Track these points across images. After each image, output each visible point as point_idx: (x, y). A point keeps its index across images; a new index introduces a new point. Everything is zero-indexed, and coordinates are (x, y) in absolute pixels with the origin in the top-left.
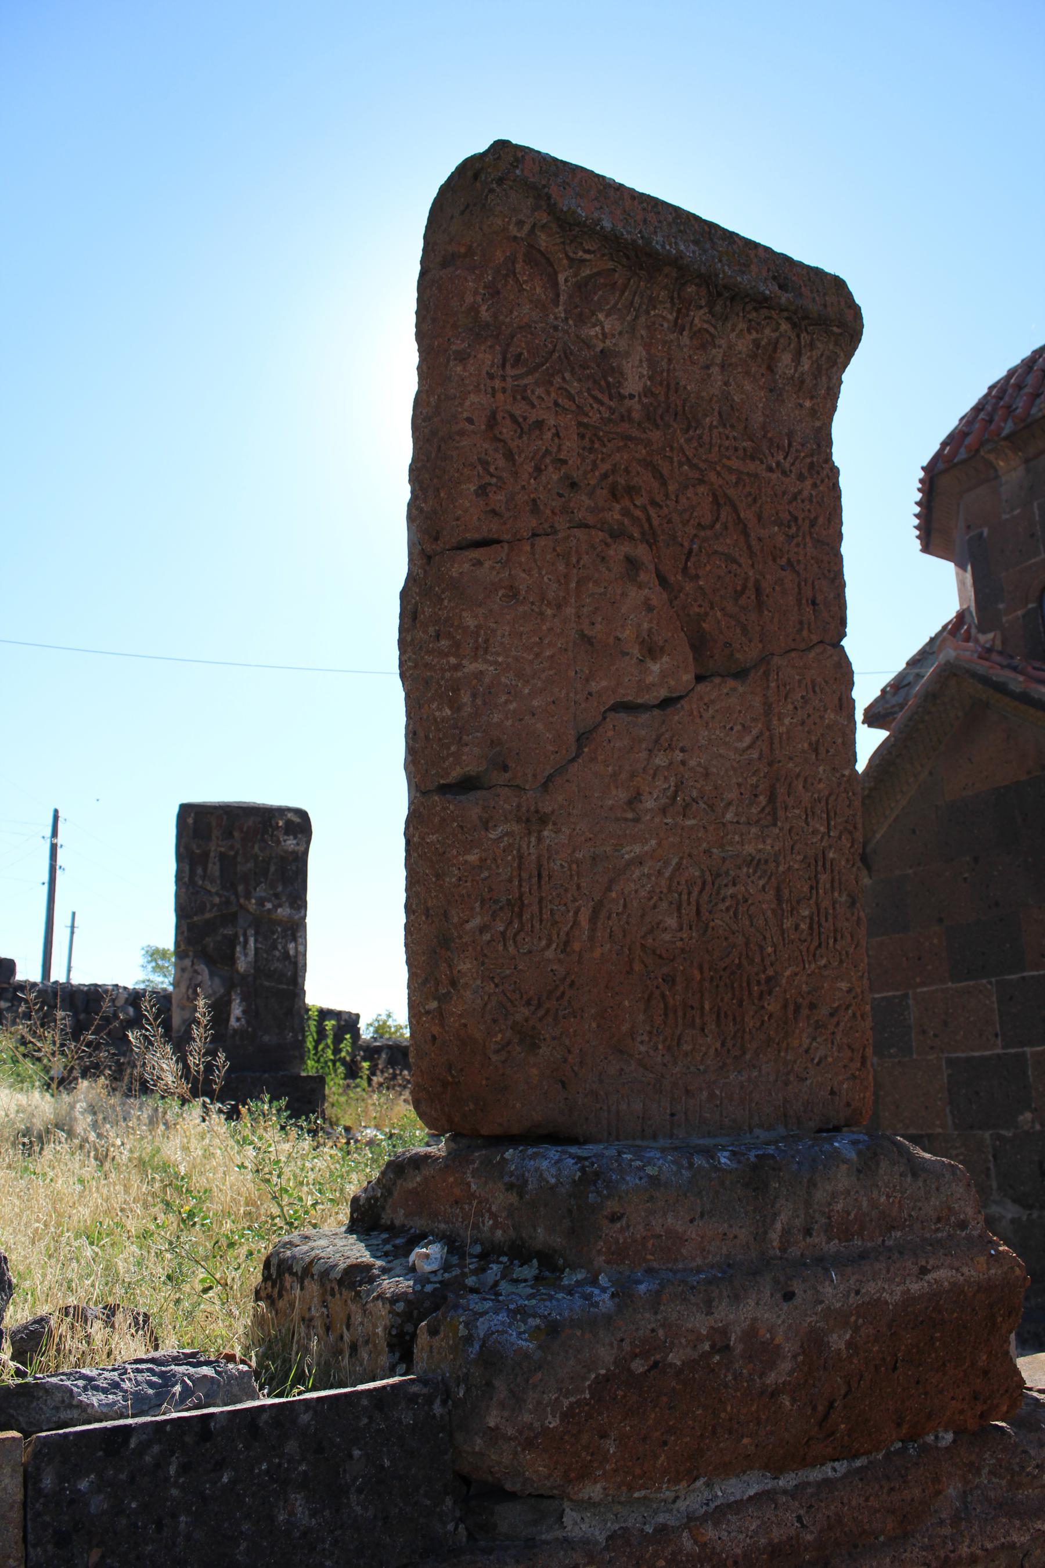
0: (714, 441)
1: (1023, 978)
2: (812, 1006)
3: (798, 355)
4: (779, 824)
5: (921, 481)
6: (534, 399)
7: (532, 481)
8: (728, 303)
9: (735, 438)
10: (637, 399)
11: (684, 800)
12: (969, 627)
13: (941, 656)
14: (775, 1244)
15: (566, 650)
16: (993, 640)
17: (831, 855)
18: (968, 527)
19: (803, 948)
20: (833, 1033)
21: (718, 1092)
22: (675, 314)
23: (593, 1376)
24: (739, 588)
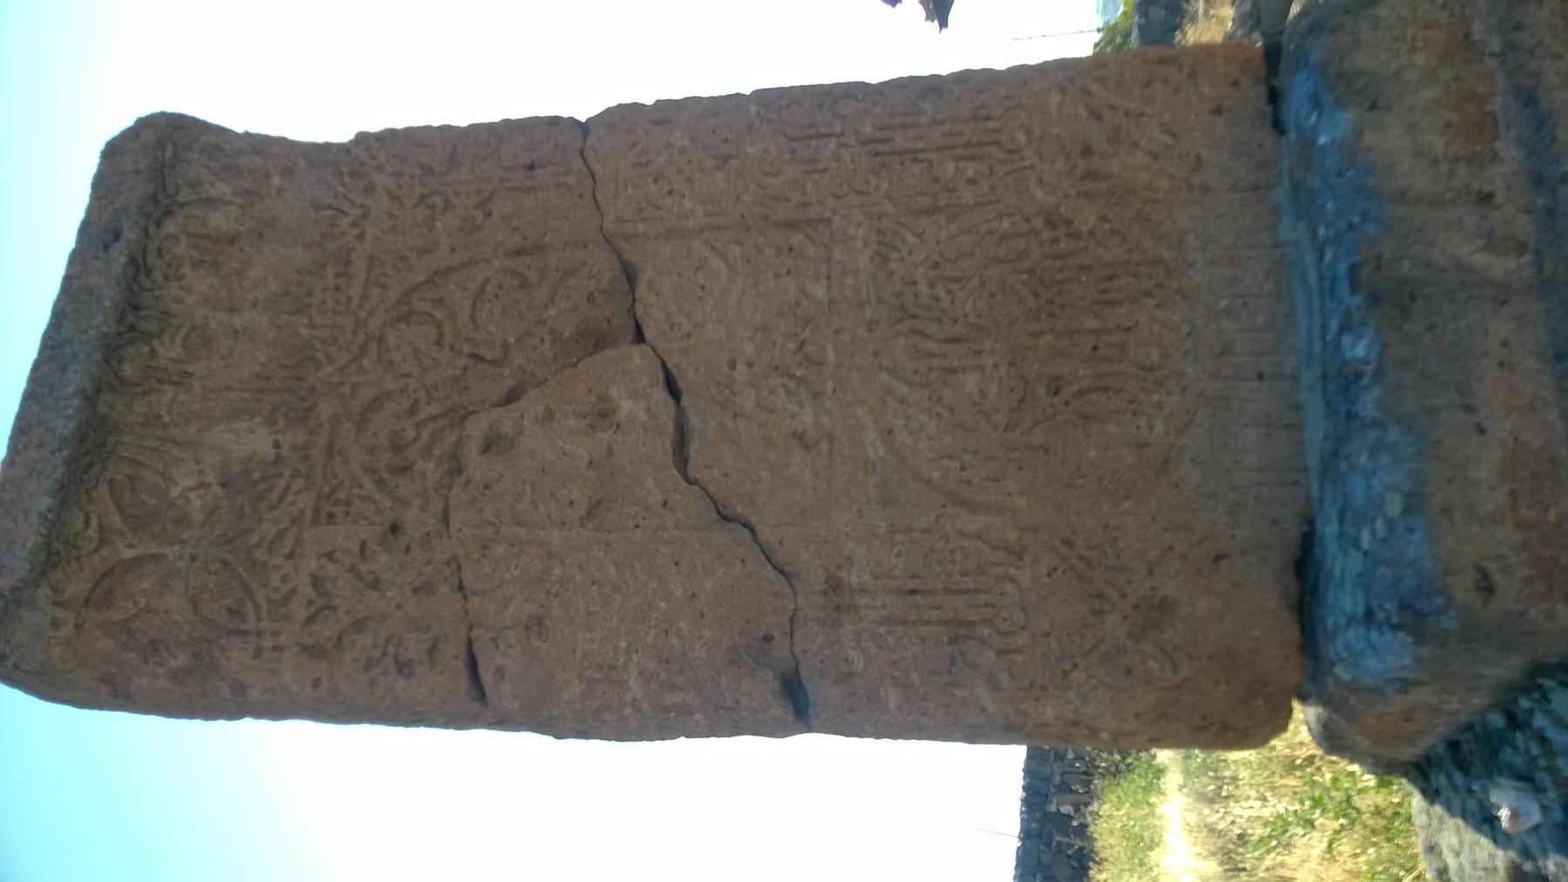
0: (329, 322)
2: (1087, 151)
3: (210, 202)
4: (827, 214)
6: (286, 588)
7: (389, 594)
8: (143, 313)
9: (325, 290)
11: (800, 364)
14: (1511, 263)
15: (607, 544)
17: (868, 130)
19: (1001, 170)
20: (1127, 114)
21: (1223, 303)
22: (166, 387)
24: (516, 282)
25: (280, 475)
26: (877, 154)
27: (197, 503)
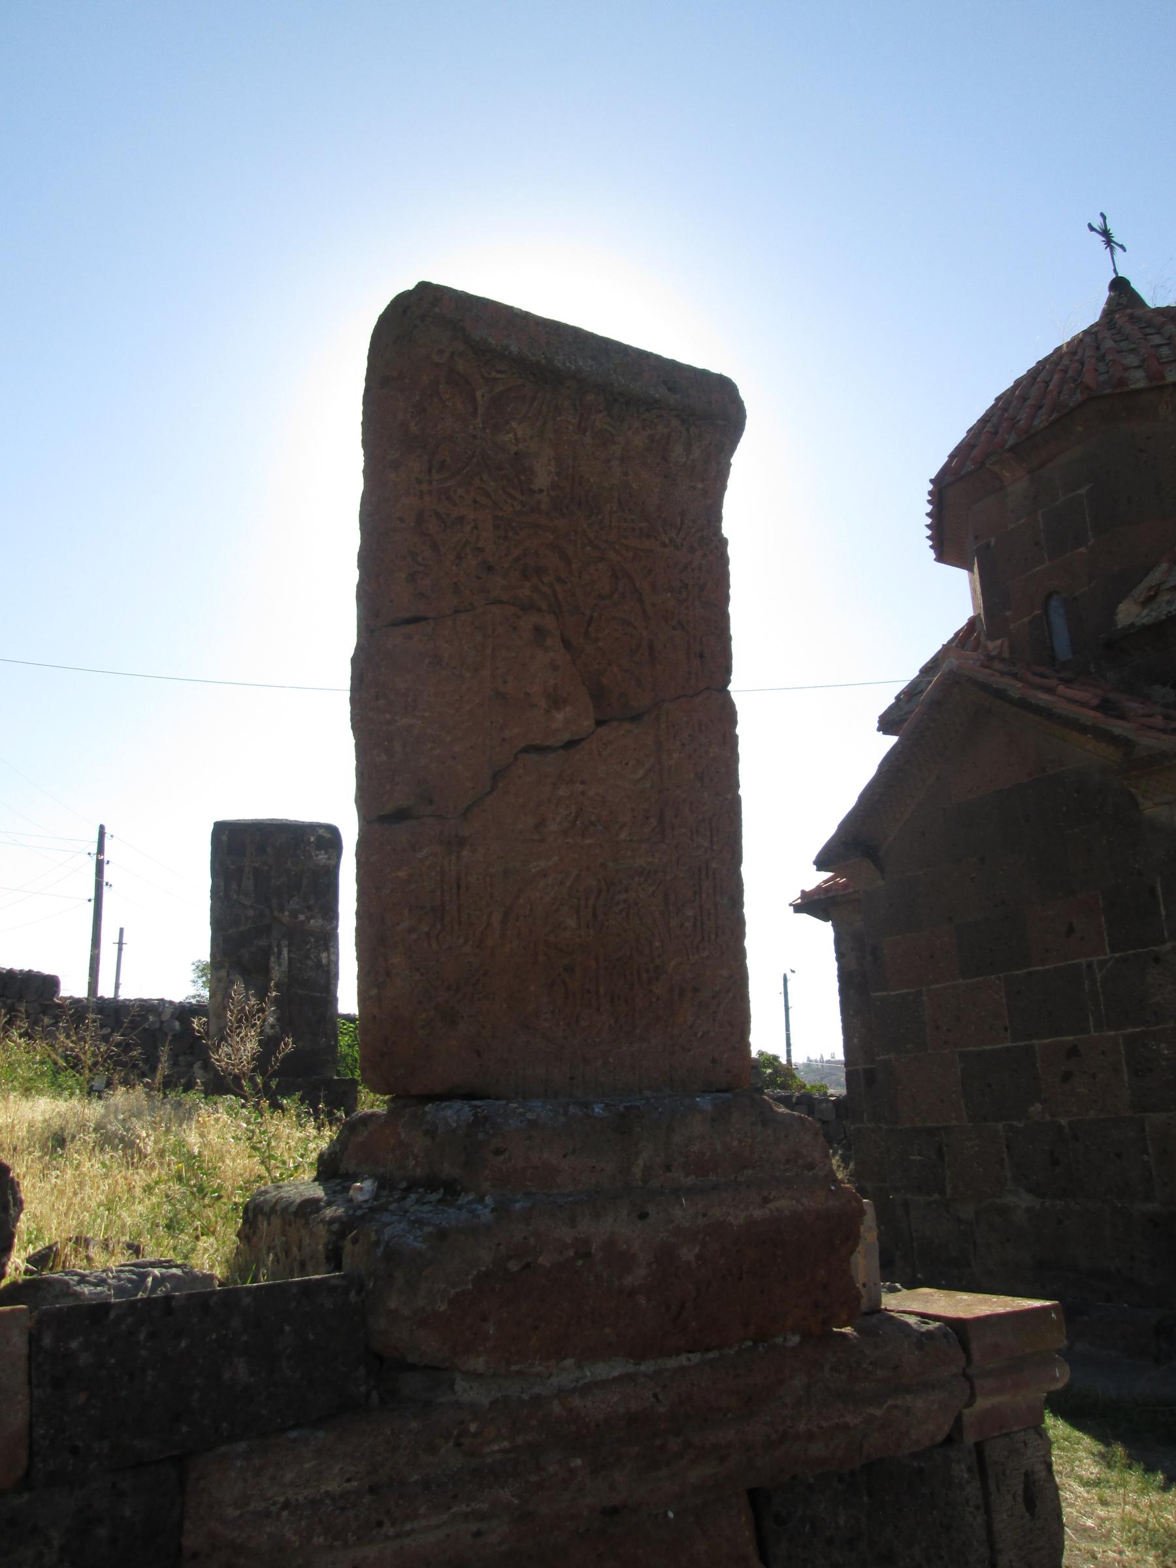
1: (1030, 973)
2: (696, 990)
5: (930, 493)
7: (454, 568)
9: (632, 520)
10: (545, 493)
12: (979, 635)
13: (944, 665)
14: (638, 1176)
16: (1001, 646)
17: (714, 865)
18: (977, 537)
20: (715, 1012)
21: (611, 1060)
22: (578, 419)
23: (475, 1273)
25: (522, 493)
26: (700, 870)
27: (506, 438)
